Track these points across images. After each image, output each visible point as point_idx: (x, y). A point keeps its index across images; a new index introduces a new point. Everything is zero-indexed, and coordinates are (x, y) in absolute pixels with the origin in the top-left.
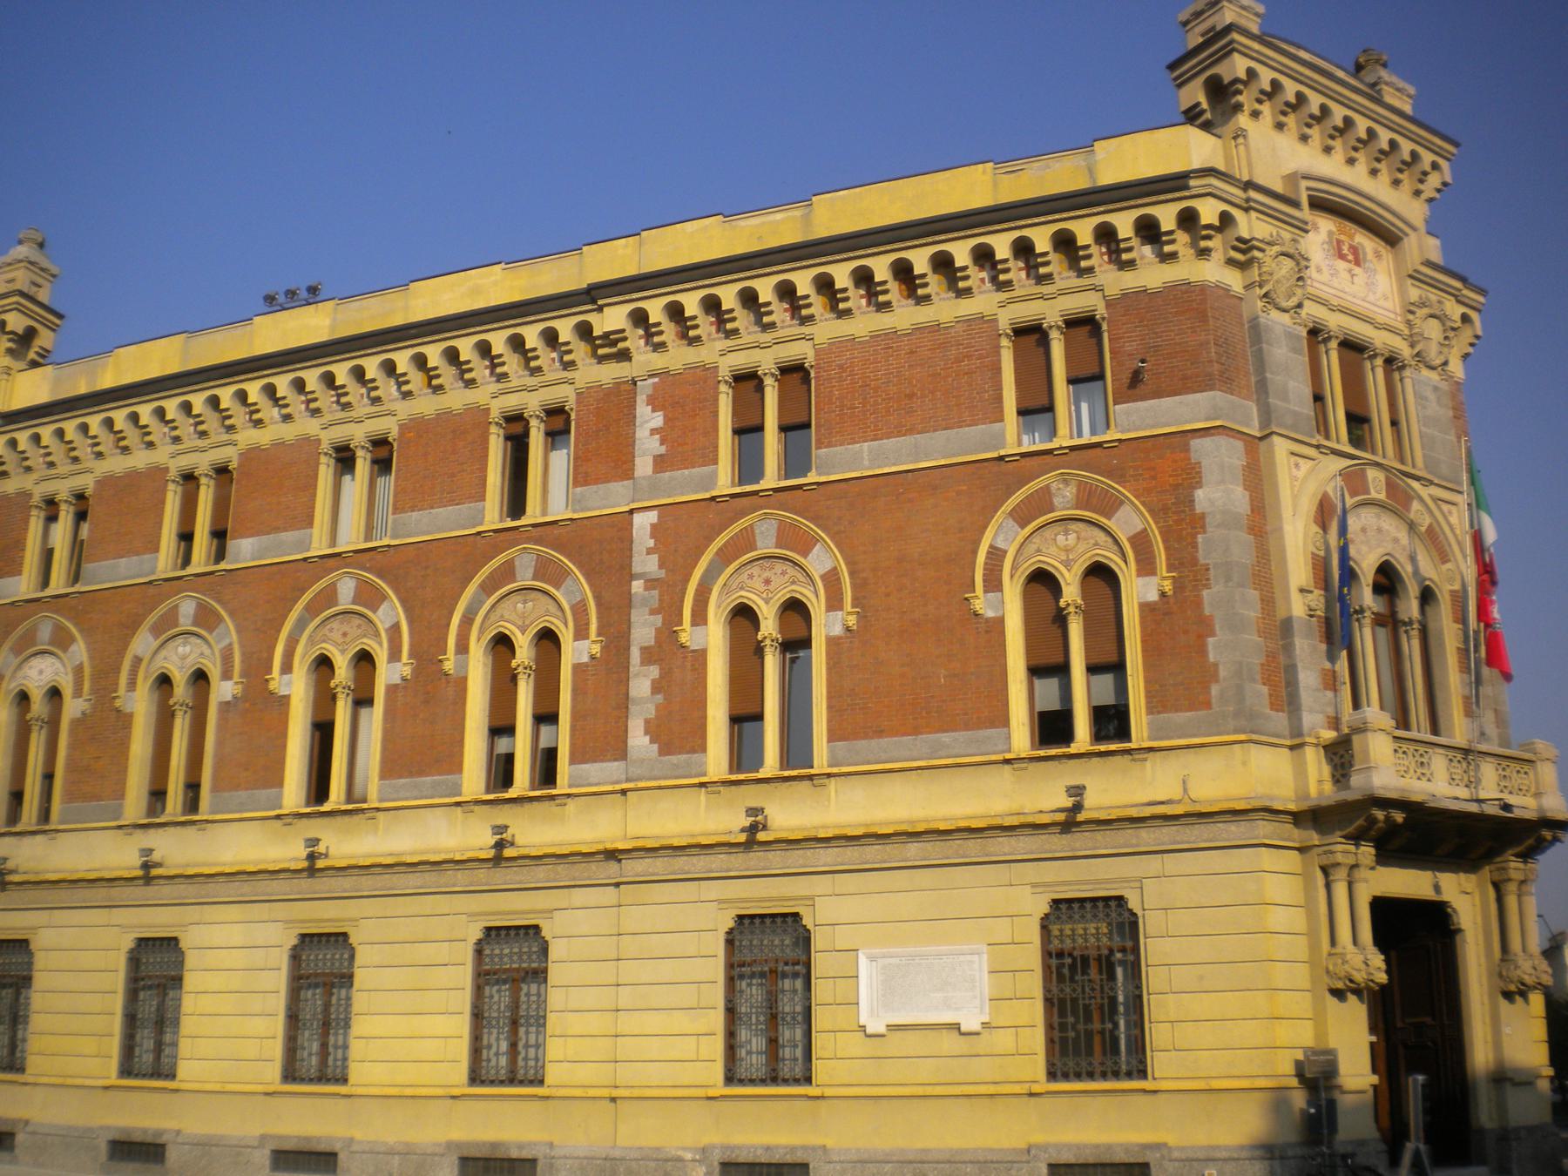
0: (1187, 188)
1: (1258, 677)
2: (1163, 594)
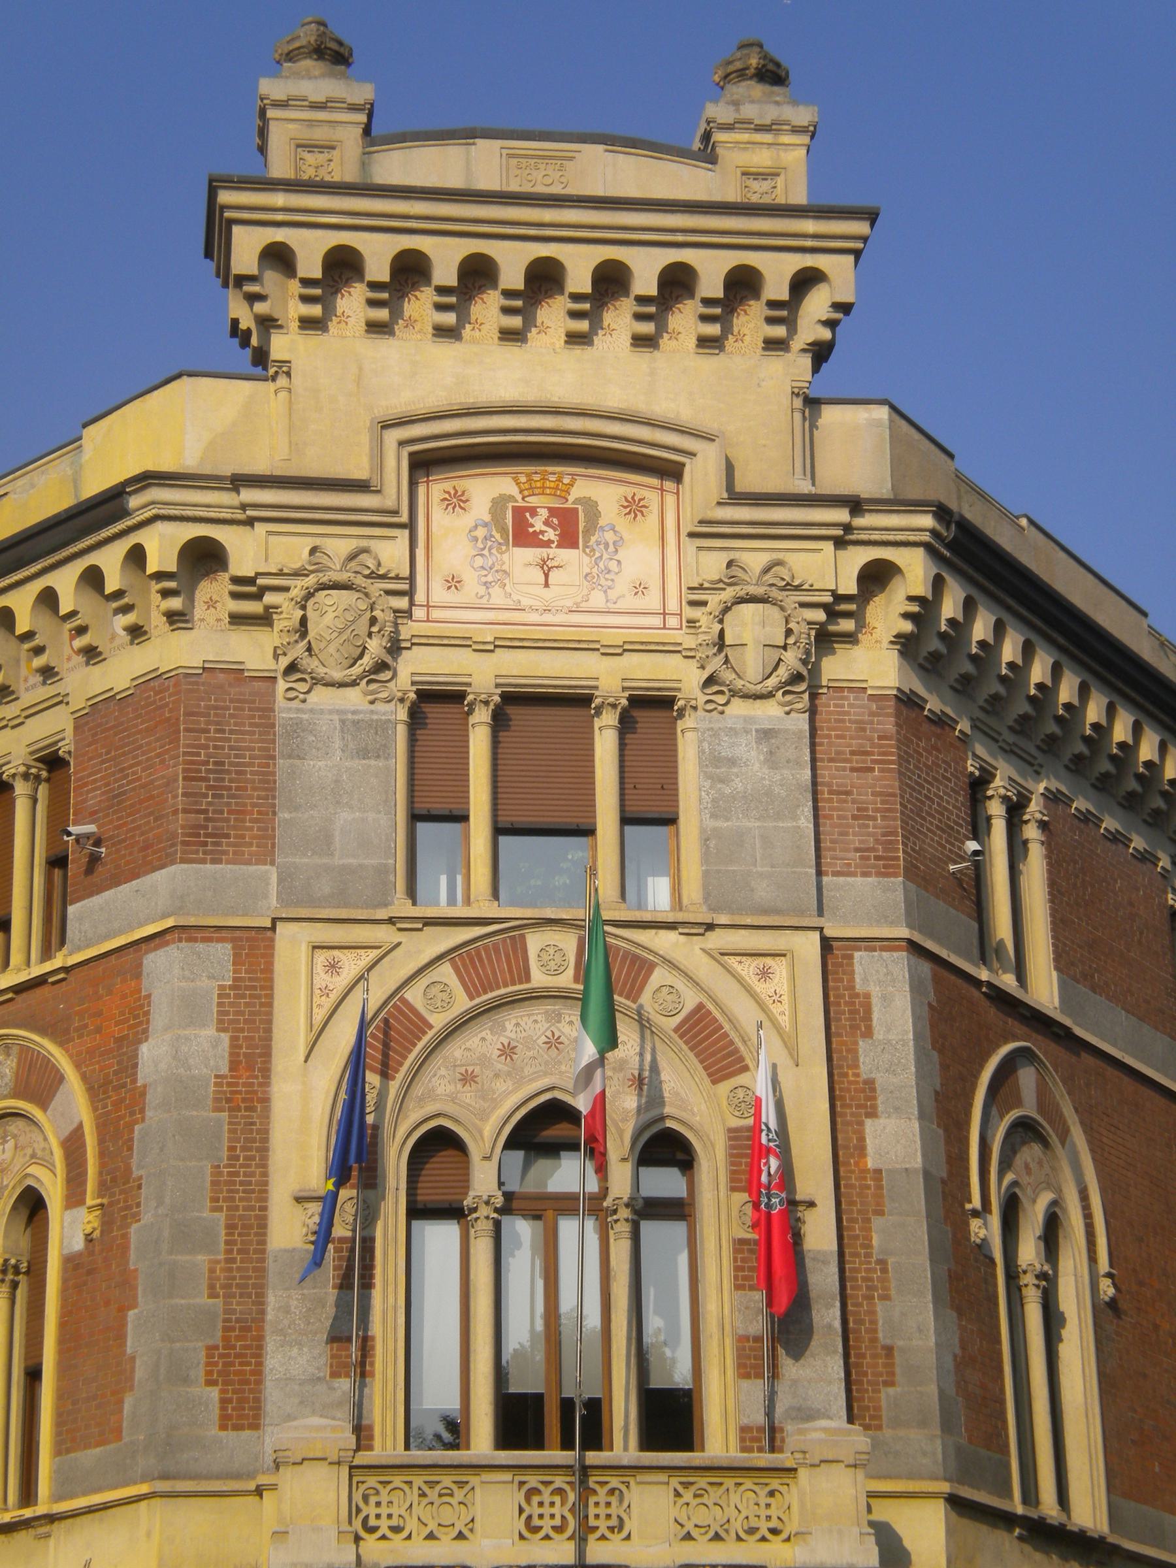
0: (125, 513)
1: (200, 1373)
2: (89, 1238)
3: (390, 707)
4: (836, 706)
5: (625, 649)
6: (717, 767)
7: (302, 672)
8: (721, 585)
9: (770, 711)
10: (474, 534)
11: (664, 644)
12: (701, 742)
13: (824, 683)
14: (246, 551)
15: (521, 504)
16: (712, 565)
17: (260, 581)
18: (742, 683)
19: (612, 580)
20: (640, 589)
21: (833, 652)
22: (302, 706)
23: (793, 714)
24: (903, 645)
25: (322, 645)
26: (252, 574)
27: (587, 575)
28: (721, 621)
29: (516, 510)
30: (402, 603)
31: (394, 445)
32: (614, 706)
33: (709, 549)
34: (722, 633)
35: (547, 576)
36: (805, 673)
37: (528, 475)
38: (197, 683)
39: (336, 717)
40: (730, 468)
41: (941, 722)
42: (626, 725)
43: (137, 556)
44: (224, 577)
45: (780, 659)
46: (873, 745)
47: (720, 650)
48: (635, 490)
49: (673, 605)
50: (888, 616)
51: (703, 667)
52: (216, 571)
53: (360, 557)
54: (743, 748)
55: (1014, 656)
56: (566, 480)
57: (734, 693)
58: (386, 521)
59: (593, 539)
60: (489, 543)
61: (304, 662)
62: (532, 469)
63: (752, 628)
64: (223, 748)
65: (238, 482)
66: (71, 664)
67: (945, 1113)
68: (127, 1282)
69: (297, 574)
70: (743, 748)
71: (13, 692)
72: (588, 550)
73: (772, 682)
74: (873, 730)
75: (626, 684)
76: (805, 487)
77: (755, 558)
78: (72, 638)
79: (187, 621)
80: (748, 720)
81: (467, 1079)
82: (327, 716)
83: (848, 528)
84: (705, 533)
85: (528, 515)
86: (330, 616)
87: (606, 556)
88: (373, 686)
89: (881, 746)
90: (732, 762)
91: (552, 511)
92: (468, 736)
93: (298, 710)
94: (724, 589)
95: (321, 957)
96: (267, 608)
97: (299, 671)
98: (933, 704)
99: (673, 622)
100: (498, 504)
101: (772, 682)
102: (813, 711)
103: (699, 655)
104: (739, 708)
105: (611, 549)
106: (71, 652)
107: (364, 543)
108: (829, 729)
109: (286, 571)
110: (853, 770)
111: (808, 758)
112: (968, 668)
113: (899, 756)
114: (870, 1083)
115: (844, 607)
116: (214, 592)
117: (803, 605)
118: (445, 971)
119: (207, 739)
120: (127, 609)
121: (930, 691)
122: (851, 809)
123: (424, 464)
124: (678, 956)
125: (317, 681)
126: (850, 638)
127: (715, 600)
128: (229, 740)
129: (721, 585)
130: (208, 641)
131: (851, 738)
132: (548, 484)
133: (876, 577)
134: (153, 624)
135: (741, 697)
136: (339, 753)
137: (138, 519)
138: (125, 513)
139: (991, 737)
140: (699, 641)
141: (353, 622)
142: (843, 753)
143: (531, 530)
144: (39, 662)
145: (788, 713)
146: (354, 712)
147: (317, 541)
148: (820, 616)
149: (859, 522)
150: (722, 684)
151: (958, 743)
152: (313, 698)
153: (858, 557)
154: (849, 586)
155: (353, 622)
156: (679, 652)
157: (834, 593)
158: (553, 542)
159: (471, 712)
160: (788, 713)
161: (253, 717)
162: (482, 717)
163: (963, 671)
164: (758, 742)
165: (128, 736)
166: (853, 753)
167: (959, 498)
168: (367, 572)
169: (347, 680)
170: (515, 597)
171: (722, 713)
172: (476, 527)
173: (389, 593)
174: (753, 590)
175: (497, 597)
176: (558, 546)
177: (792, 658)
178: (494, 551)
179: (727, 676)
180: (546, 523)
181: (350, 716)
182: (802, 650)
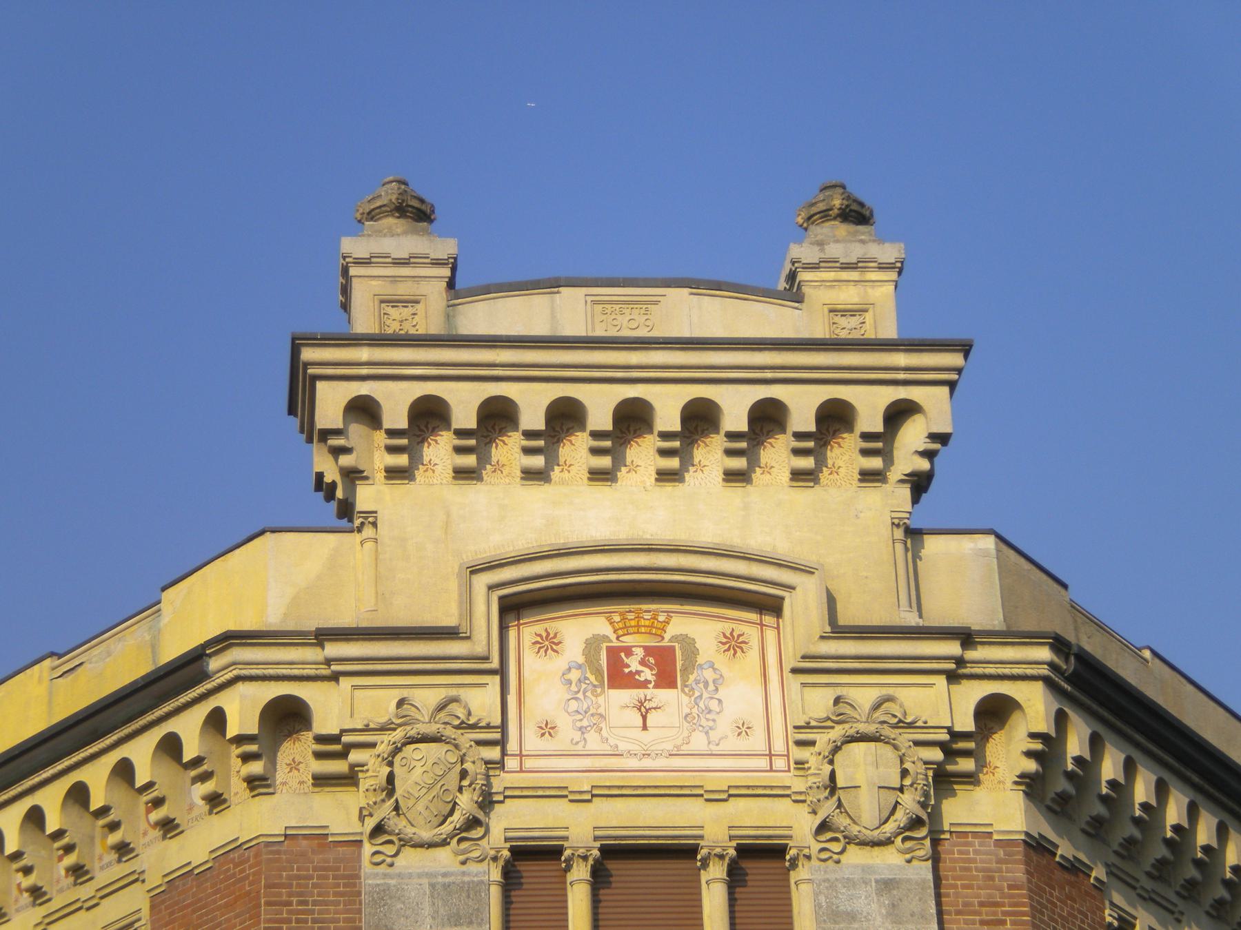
0: (205, 676)
3: (483, 867)
4: (960, 852)
5: (731, 794)
6: (836, 922)
7: (390, 833)
8: (829, 723)
9: (890, 859)
10: (567, 677)
11: (772, 787)
12: (816, 895)
13: (946, 828)
14: (330, 708)
15: (616, 644)
16: (818, 702)
17: (345, 739)
18: (858, 828)
19: (714, 720)
20: (743, 729)
21: (953, 794)
22: (390, 870)
23: (915, 863)
24: (1027, 785)
25: (411, 803)
26: (337, 732)
27: (687, 716)
28: (831, 762)
29: (609, 649)
30: (494, 753)
31: (484, 590)
32: (721, 857)
33: (814, 685)
34: (833, 776)
35: (644, 718)
36: (925, 817)
37: (621, 614)
38: (278, 852)
39: (425, 881)
40: (831, 601)
41: (1074, 868)
42: (735, 878)
43: (217, 720)
44: (308, 737)
45: (897, 802)
46: (1003, 896)
47: (832, 793)
48: (734, 626)
49: (779, 746)
50: (1009, 754)
51: (814, 812)
52: (300, 730)
53: (450, 707)
54: (862, 901)
55: (1147, 796)
56: (661, 618)
57: (850, 840)
58: (476, 668)
59: (692, 678)
60: (584, 686)
61: (391, 822)
62: (627, 607)
63: (864, 768)
64: (306, 921)
65: (323, 636)
66: (147, 839)
69: (383, 729)
70: (862, 901)
71: (87, 872)
72: (686, 690)
73: (890, 827)
74: (1002, 879)
75: (733, 833)
76: (912, 619)
77: (863, 694)
78: (148, 811)
79: (268, 786)
80: (866, 869)
82: (416, 881)
83: (960, 661)
84: (809, 668)
85: (623, 655)
86: (418, 771)
87: (705, 695)
88: (464, 845)
89: (1012, 896)
91: (648, 650)
92: (566, 895)
93: (385, 876)
94: (832, 728)
96: (352, 766)
97: (385, 832)
98: (1065, 849)
99: (780, 763)
100: (592, 645)
101: (890, 827)
102: (936, 859)
103: (809, 799)
104: (856, 857)
105: (711, 687)
106: (146, 825)
107: (453, 692)
108: (954, 878)
109: (372, 726)
110: (983, 923)
111: (933, 911)
112: (1100, 809)
113: (1032, 906)
115: (962, 745)
116: (297, 752)
117: (918, 743)
119: (289, 912)
120: (205, 777)
121: (1060, 836)
123: (514, 607)
125: (406, 842)
126: (970, 779)
127: (824, 740)
128: (312, 912)
129: (829, 723)
130: (293, 805)
131: (979, 888)
132: (642, 622)
133: (994, 713)
134: (233, 791)
135: (857, 844)
136: (429, 920)
137: (219, 681)
138: (205, 676)
139: (1129, 884)
140: (810, 784)
141: (443, 776)
142: (971, 904)
143: (627, 670)
144: (114, 838)
145: (909, 861)
146: (445, 875)
147: (405, 693)
148: (937, 755)
149: (971, 655)
150: (837, 830)
151: (1094, 892)
152: (400, 861)
153: (973, 693)
154: (966, 723)
155: (443, 776)
156: (788, 796)
157: (950, 731)
158: (650, 682)
159: (568, 868)
160: (909, 861)
161: (338, 885)
162: (580, 873)
163: (1094, 813)
164: (879, 893)
165: (206, 914)
166: (982, 904)
167: (1076, 629)
168: (457, 722)
169: (437, 839)
170: (612, 741)
171: (838, 862)
172: (570, 669)
173: (479, 743)
174: (863, 728)
175: (593, 742)
176: (657, 686)
177: (909, 802)
178: (589, 694)
179: (842, 821)
180: (643, 662)
181: (440, 879)
182: (919, 792)
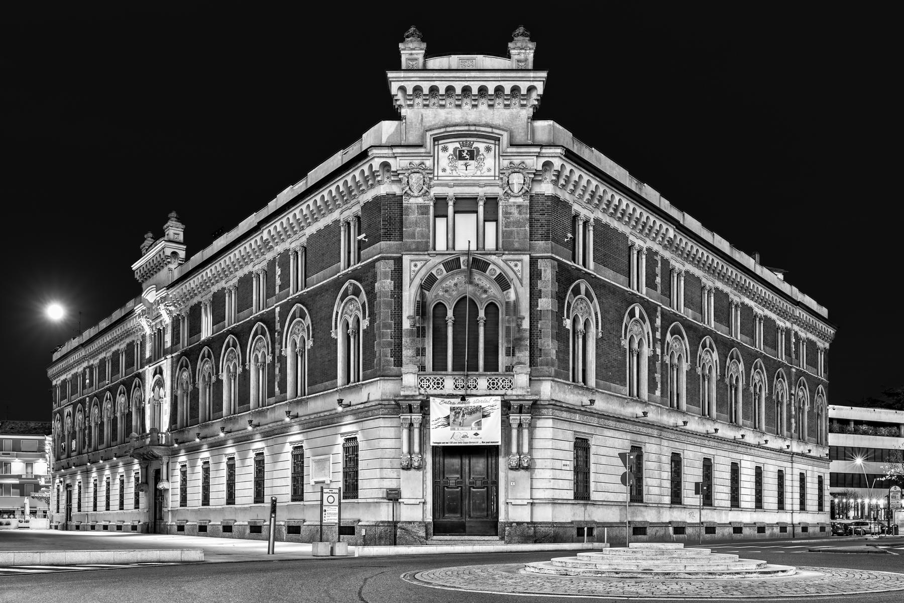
5: (485, 186)
14: (395, 165)
16: (505, 163)
20: (489, 170)
49: (497, 174)
58: (428, 155)
63: (517, 180)
67: (560, 297)
68: (374, 336)
77: (517, 160)
81: (446, 291)
90: (510, 213)
95: (413, 264)
100: (455, 149)
104: (512, 200)
114: (540, 291)
118: (442, 267)
122: (539, 224)
124: (496, 261)
133: (547, 165)
153: (543, 160)
154: (540, 168)
175: (454, 173)
